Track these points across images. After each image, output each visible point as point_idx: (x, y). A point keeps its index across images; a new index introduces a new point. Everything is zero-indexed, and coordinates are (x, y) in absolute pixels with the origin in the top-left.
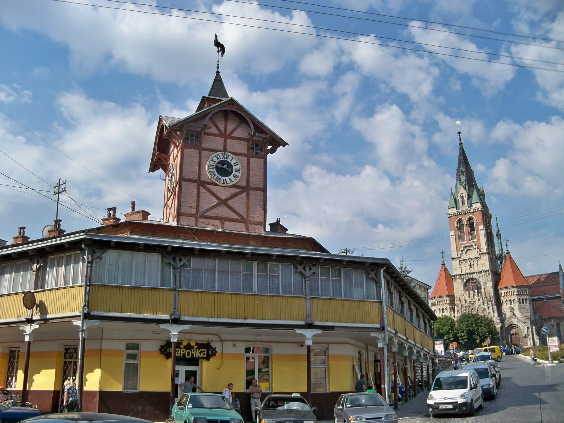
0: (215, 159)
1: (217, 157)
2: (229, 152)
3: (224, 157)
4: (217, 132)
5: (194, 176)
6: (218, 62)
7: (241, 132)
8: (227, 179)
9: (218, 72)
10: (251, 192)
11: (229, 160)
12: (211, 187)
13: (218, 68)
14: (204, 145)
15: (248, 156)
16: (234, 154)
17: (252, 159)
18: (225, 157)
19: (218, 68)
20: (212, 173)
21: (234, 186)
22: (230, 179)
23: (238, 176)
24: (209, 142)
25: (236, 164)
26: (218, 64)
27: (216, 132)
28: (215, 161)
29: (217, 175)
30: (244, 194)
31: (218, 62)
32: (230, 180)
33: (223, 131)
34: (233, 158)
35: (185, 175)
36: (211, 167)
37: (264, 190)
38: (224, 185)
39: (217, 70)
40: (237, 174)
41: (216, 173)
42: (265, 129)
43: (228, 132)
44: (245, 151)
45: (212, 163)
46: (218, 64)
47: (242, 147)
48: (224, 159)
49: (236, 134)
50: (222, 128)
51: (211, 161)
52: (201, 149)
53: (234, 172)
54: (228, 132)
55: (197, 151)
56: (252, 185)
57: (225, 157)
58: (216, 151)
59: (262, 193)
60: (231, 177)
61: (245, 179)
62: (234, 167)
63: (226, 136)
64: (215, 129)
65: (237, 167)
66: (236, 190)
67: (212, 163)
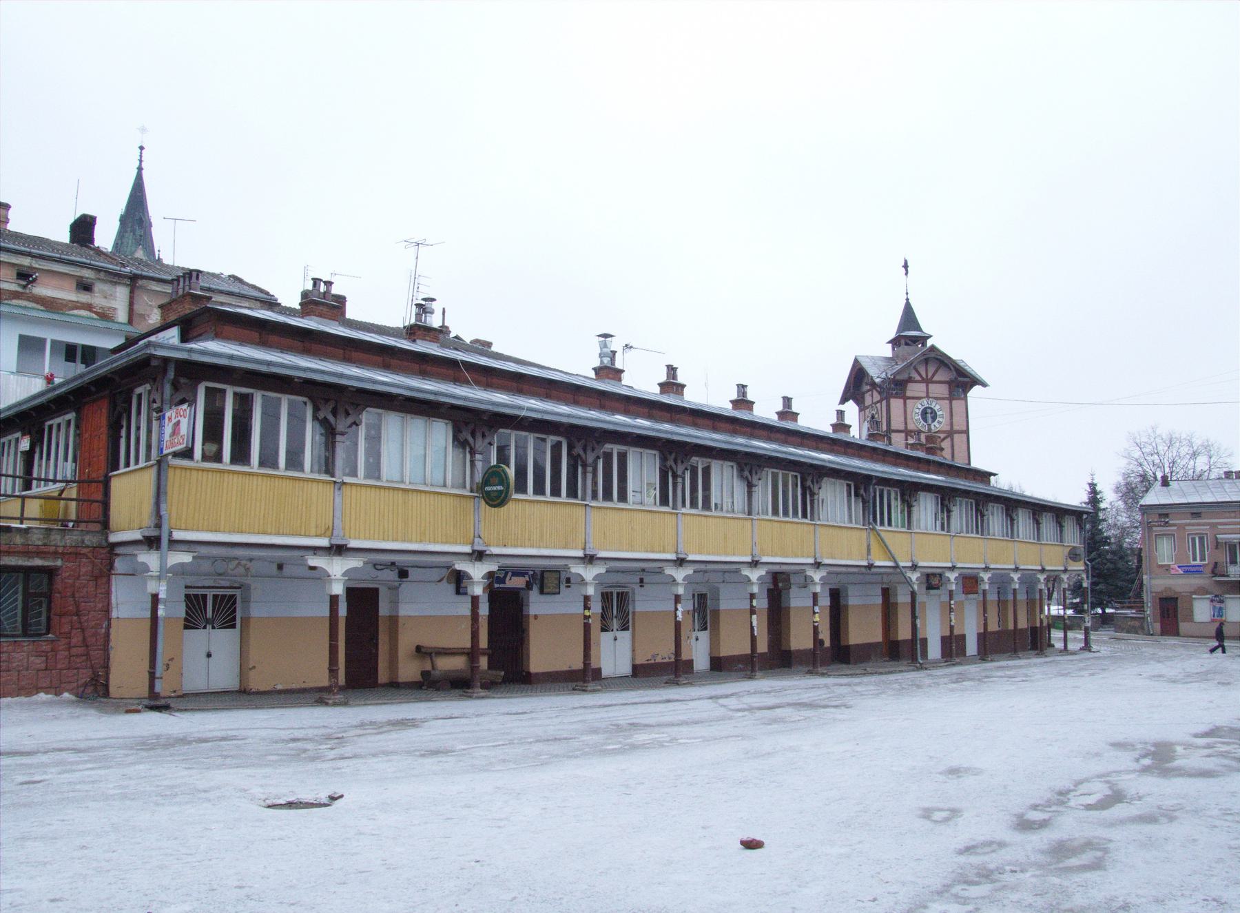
0: (920, 406)
2: (932, 398)
4: (918, 378)
5: (902, 428)
7: (942, 375)
9: (907, 299)
10: (956, 436)
13: (907, 294)
14: (909, 394)
15: (951, 398)
16: (936, 398)
17: (954, 402)
19: (907, 294)
24: (914, 389)
29: (923, 422)
30: (948, 440)
33: (924, 376)
35: (893, 427)
37: (967, 432)
40: (941, 420)
42: (966, 373)
43: (929, 377)
45: (917, 411)
47: (942, 390)
49: (936, 378)
50: (924, 376)
52: (905, 398)
53: (938, 419)
54: (929, 377)
55: (902, 401)
56: (956, 428)
59: (964, 436)
60: (936, 423)
62: (938, 413)
63: (927, 381)
65: (941, 413)
67: (917, 411)
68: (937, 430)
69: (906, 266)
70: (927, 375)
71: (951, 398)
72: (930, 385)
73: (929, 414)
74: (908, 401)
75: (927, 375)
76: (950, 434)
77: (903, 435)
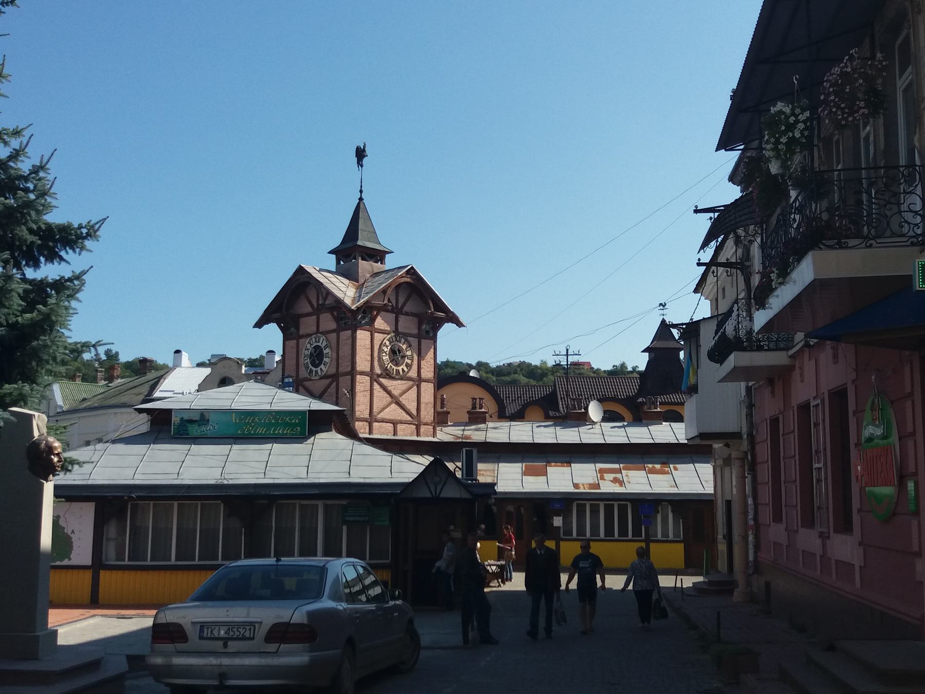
0: (309, 345)
1: (311, 344)
2: (321, 333)
3: (316, 339)
4: (309, 309)
6: (361, 182)
8: (319, 369)
9: (361, 199)
12: (307, 384)
13: (361, 191)
14: (302, 332)
18: (317, 340)
19: (361, 191)
21: (325, 377)
22: (321, 369)
23: (327, 363)
25: (326, 347)
26: (361, 187)
27: (309, 309)
28: (309, 349)
29: (311, 367)
31: (361, 182)
34: (323, 340)
36: (306, 358)
38: (315, 378)
39: (359, 197)
41: (310, 365)
44: (333, 325)
45: (306, 352)
46: (361, 187)
48: (316, 344)
51: (306, 350)
55: (295, 342)
57: (317, 340)
58: (309, 335)
60: (322, 366)
61: (334, 363)
62: (325, 352)
64: (309, 305)
66: (327, 381)
67: (306, 352)
68: (323, 374)
69: (360, 154)
71: (337, 331)
73: (317, 356)
74: (301, 341)
76: (334, 378)
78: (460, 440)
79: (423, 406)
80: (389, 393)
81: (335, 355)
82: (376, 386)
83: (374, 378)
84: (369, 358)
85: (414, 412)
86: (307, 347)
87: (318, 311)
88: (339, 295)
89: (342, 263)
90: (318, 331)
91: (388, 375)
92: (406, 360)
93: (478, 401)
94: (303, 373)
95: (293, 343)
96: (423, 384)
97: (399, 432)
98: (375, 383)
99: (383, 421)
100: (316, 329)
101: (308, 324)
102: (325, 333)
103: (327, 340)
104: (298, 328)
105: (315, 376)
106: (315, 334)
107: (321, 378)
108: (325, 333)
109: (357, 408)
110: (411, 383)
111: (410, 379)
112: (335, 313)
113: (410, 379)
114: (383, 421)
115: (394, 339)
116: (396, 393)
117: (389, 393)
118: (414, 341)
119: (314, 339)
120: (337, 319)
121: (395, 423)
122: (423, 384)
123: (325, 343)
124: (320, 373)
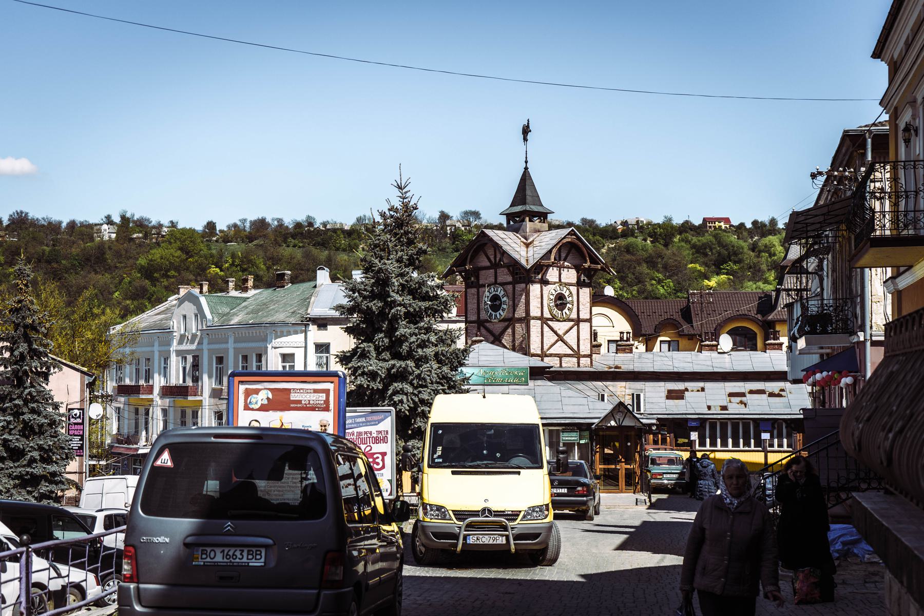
4: (488, 264)
8: (498, 313)
9: (526, 168)
11: (498, 293)
12: (487, 325)
13: (526, 162)
19: (526, 162)
20: (487, 311)
21: (504, 320)
26: (526, 158)
27: (486, 263)
29: (490, 311)
32: (502, 314)
33: (493, 260)
40: (505, 306)
44: (509, 279)
46: (526, 158)
48: (494, 293)
53: (503, 306)
55: (475, 290)
58: (489, 285)
60: (501, 311)
62: (503, 300)
65: (505, 299)
68: (502, 318)
69: (526, 131)
70: (495, 260)
71: (514, 283)
72: (499, 271)
75: (495, 260)
77: (476, 325)
78: (613, 370)
79: (581, 342)
80: (555, 332)
81: (511, 303)
82: (546, 328)
83: (543, 320)
84: (540, 306)
85: (575, 348)
86: (487, 294)
87: (495, 266)
88: (516, 256)
89: (512, 223)
90: (496, 283)
91: (554, 318)
92: (568, 305)
93: (625, 334)
94: (483, 316)
95: (474, 291)
96: (582, 324)
97: (564, 365)
98: (545, 325)
99: (551, 355)
100: (494, 281)
101: (487, 276)
102: (502, 284)
103: (505, 290)
104: (478, 278)
105: (495, 319)
106: (493, 284)
107: (500, 321)
108: (502, 284)
109: (532, 347)
110: (572, 323)
111: (572, 320)
112: (511, 269)
113: (572, 320)
114: (551, 355)
115: (558, 289)
116: (561, 333)
117: (555, 332)
118: (574, 289)
119: (492, 289)
120: (513, 274)
121: (560, 356)
122: (582, 324)
123: (502, 293)
124: (498, 317)
